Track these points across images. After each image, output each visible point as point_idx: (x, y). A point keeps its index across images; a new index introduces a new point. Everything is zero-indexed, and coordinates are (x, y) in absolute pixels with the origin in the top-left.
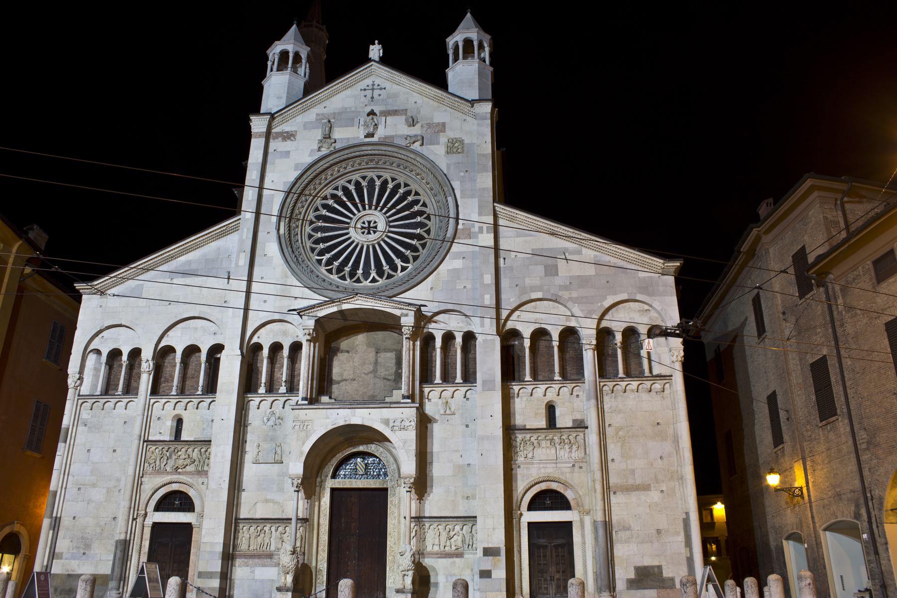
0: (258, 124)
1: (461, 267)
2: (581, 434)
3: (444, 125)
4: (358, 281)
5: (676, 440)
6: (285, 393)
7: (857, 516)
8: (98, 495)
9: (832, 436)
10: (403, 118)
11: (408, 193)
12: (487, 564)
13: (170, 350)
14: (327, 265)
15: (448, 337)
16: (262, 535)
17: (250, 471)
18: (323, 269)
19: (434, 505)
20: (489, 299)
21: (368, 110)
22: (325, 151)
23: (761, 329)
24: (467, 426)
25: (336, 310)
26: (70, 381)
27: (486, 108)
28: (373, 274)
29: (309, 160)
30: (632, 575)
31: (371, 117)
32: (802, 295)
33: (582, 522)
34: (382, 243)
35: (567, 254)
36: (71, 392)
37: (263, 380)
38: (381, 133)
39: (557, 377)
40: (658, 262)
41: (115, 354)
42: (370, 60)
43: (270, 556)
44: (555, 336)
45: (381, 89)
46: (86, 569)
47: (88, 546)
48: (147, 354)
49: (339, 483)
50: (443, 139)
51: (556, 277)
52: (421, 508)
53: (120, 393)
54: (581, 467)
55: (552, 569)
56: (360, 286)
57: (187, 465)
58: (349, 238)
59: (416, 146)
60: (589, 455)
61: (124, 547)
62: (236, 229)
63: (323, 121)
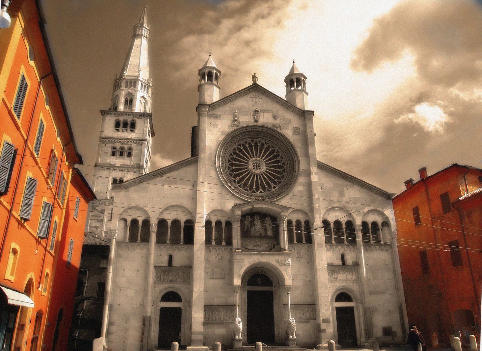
1: (303, 189)
2: (356, 269)
3: (290, 120)
4: (254, 192)
6: (225, 245)
10: (272, 114)
14: (238, 183)
15: (298, 222)
16: (217, 313)
18: (237, 185)
21: (254, 108)
24: (308, 263)
25: (251, 207)
28: (261, 189)
31: (257, 112)
33: (358, 307)
34: (263, 174)
35: (348, 187)
37: (214, 238)
41: (134, 222)
45: (260, 98)
48: (154, 224)
50: (290, 127)
51: (343, 197)
53: (140, 241)
54: (357, 283)
56: (255, 195)
57: (177, 279)
58: (248, 170)
59: (278, 130)
60: (360, 277)
63: (233, 111)
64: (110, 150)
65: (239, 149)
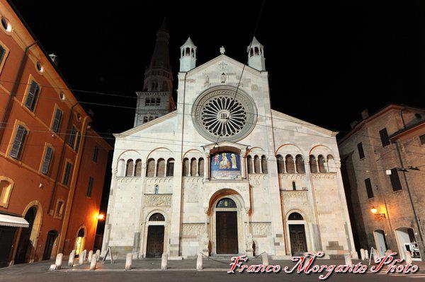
0: (181, 76)
4: (221, 135)
5: (340, 196)
7: (412, 226)
11: (237, 104)
12: (277, 240)
13: (152, 159)
15: (256, 157)
17: (186, 205)
19: (255, 218)
20: (271, 144)
23: (362, 156)
27: (266, 74)
28: (227, 133)
32: (384, 145)
36: (113, 175)
38: (227, 82)
39: (296, 172)
41: (130, 161)
42: (220, 54)
43: (195, 237)
44: (294, 157)
46: (123, 244)
47: (123, 235)
48: (144, 162)
49: (219, 209)
52: (250, 219)
55: (298, 242)
64: (142, 119)
65: (210, 104)
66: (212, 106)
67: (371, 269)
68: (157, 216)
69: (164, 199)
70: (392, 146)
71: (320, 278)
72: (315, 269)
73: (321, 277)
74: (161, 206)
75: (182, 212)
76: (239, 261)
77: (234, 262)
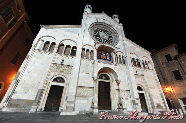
8: (35, 75)
9: (181, 83)
13: (63, 45)
15: (119, 56)
17: (81, 74)
19: (122, 87)
22: (96, 22)
26: (33, 45)
29: (94, 22)
30: (156, 106)
36: (32, 47)
40: (148, 52)
41: (48, 43)
43: (85, 97)
47: (28, 90)
61: (41, 92)
62: (81, 27)
66: (98, 30)
67: (162, 117)
68: (60, 79)
69: (67, 68)
70: (174, 62)
71: (140, 121)
72: (138, 117)
73: (140, 121)
74: (64, 73)
75: (78, 79)
76: (105, 114)
77: (102, 114)
